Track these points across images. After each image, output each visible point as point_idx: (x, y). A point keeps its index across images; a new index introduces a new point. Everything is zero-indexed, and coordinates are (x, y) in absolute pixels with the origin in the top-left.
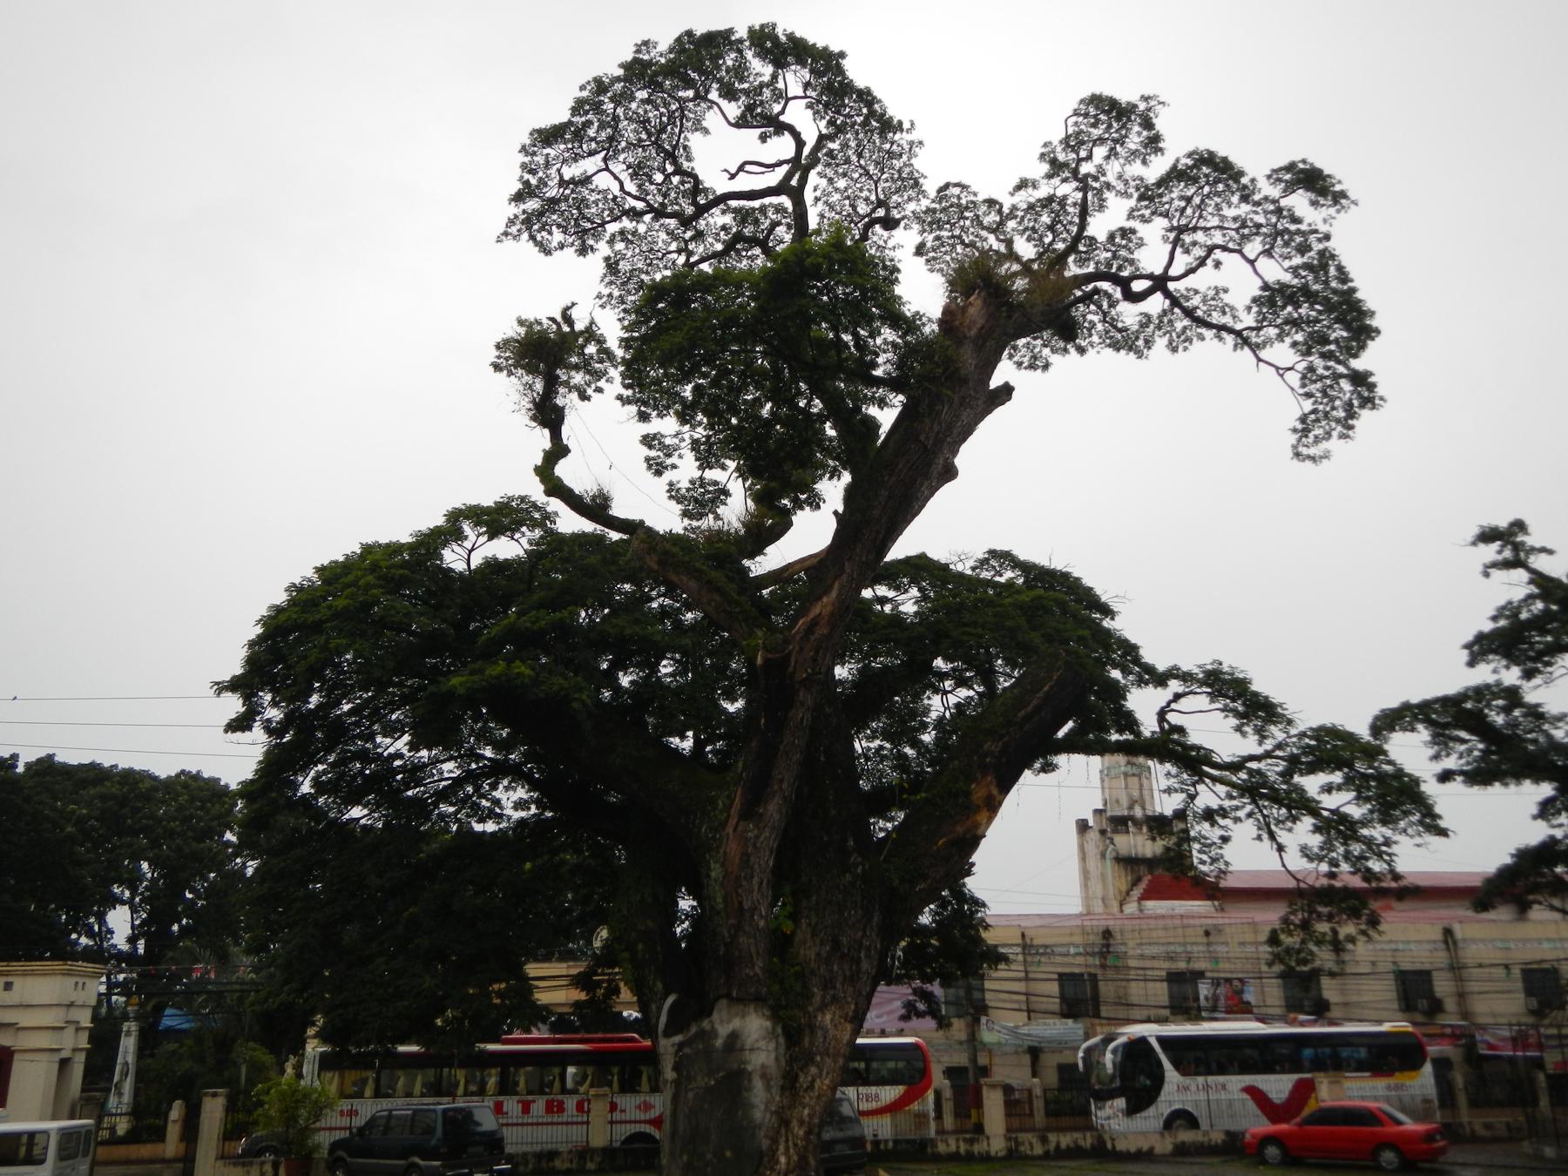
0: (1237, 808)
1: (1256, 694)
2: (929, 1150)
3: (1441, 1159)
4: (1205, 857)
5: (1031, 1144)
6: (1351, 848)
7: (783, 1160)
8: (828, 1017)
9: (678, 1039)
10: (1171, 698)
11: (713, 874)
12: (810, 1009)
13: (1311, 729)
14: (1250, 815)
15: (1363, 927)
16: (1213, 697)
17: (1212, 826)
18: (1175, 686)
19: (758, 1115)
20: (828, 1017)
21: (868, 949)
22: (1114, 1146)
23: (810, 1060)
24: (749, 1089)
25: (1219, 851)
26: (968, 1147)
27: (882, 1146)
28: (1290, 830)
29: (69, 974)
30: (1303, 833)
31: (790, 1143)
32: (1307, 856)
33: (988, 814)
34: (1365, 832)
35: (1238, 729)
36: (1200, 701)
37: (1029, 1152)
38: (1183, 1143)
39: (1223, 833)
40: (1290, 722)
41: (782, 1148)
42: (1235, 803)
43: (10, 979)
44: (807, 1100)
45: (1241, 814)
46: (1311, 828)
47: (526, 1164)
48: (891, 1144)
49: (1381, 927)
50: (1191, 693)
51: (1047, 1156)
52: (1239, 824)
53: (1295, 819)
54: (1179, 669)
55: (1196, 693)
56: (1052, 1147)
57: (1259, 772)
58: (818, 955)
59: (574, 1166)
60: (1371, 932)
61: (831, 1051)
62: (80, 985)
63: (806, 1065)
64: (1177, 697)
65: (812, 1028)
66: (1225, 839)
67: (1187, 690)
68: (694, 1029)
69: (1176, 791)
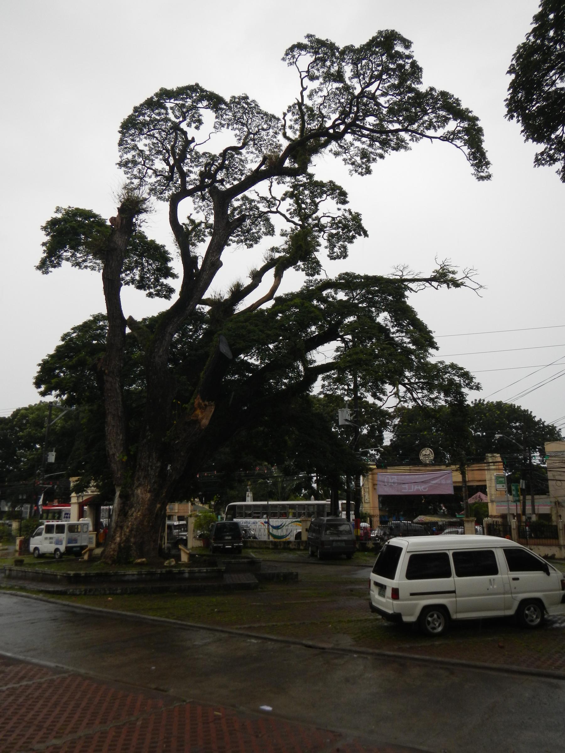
7: (118, 539)
8: (139, 491)
20: (139, 491)
21: (151, 466)
23: (132, 506)
31: (123, 534)
41: (118, 535)
44: (130, 519)
47: (280, 545)
59: (296, 547)
61: (140, 503)
65: (133, 494)
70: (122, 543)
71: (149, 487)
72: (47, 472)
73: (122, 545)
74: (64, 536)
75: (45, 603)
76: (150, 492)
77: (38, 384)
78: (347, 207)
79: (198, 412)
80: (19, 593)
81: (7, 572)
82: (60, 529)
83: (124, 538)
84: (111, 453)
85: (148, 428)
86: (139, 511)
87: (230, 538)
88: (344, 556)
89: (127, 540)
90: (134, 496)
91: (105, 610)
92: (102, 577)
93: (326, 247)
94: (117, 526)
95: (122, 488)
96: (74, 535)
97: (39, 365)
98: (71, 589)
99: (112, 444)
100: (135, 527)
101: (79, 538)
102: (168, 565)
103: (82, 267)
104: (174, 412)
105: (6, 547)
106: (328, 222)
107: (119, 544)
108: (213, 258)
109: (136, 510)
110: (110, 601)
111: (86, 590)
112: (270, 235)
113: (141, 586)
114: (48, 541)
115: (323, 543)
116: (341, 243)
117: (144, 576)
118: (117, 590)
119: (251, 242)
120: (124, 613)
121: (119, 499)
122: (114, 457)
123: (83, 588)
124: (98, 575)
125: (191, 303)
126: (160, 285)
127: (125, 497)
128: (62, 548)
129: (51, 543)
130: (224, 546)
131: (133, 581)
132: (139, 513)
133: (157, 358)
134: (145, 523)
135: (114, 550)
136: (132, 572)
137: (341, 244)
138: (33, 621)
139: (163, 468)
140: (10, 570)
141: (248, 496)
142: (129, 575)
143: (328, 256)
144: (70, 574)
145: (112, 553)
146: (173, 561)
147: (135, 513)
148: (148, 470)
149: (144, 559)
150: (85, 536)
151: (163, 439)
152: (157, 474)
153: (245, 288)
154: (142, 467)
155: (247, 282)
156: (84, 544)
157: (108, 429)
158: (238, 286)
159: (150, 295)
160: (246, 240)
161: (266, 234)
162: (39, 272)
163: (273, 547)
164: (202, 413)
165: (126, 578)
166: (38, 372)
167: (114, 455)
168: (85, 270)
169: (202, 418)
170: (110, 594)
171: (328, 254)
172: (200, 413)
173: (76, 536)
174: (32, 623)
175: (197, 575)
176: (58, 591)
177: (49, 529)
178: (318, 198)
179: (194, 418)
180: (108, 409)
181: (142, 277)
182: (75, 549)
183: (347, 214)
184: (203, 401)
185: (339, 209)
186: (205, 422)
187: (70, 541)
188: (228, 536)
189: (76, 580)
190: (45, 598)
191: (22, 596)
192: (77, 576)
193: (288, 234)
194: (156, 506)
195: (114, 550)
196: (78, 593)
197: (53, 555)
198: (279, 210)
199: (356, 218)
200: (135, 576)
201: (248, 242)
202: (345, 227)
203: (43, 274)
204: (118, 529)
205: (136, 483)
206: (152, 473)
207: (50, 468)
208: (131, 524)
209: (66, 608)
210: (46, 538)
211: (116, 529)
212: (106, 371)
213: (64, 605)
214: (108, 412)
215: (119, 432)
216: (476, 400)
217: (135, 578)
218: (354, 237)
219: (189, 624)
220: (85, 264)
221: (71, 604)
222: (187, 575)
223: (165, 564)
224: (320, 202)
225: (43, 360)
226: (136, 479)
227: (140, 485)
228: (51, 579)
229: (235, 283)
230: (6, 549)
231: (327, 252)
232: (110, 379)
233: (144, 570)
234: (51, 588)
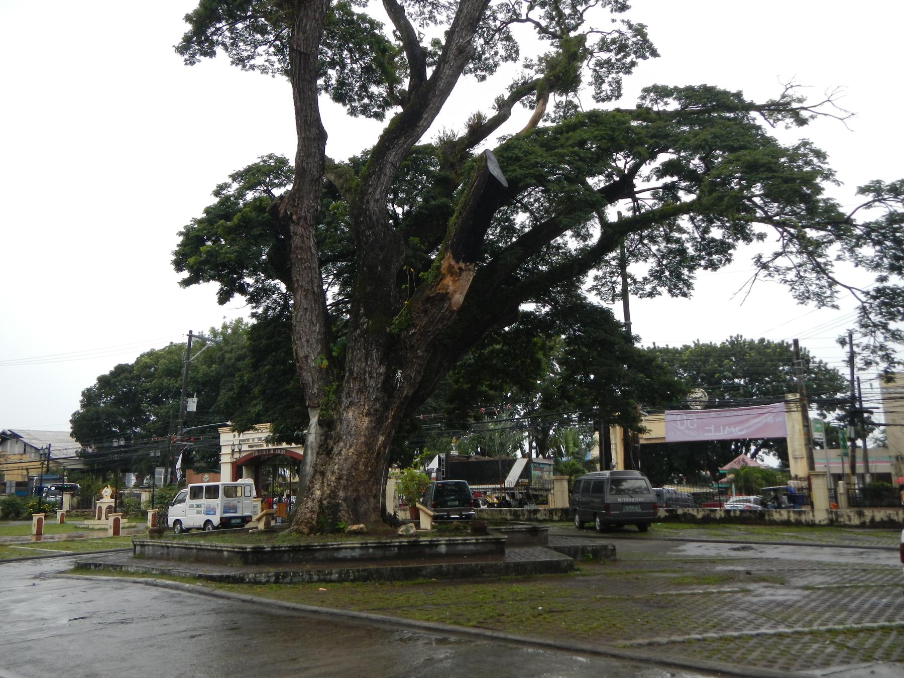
2: (767, 518)
5: (849, 517)
8: (350, 414)
12: (341, 410)
20: (350, 414)
21: (370, 373)
23: (339, 439)
26: (796, 516)
27: (732, 514)
31: (325, 484)
37: (847, 522)
41: (317, 486)
47: (524, 515)
48: (738, 513)
51: (863, 525)
56: (868, 520)
59: (547, 518)
61: (353, 433)
63: (338, 441)
70: (325, 499)
71: (367, 407)
72: (185, 424)
73: (325, 502)
74: (218, 503)
75: (209, 598)
76: (368, 415)
77: (179, 265)
78: (625, 15)
79: (448, 281)
80: (159, 581)
81: (138, 548)
82: (212, 492)
83: (328, 492)
84: (302, 354)
86: (351, 446)
87: (457, 503)
88: (634, 528)
89: (333, 495)
90: (341, 423)
91: (325, 609)
92: (300, 553)
93: (590, 84)
94: (315, 471)
95: (322, 410)
96: (232, 501)
97: (181, 234)
98: (251, 573)
99: (304, 340)
100: (345, 472)
101: (239, 505)
102: (404, 533)
103: (247, 67)
104: (404, 286)
105: (133, 524)
106: (594, 44)
107: (320, 501)
108: (461, 41)
109: (346, 445)
110: (323, 592)
111: (277, 575)
112: (512, 59)
113: (372, 567)
114: (194, 510)
115: (607, 507)
116: (614, 75)
117: (371, 550)
118: (331, 574)
119: (483, 73)
120: (363, 615)
121: (318, 427)
122: (307, 360)
123: (272, 571)
124: (295, 550)
125: (425, 116)
126: (369, 97)
127: (327, 424)
128: (216, 520)
129: (198, 513)
130: (448, 515)
131: (353, 560)
132: (352, 450)
133: (372, 204)
134: (362, 467)
135: (312, 512)
136: (350, 546)
137: (613, 78)
138: (194, 633)
139: (389, 377)
140: (142, 546)
142: (346, 548)
143: (594, 97)
144: (246, 548)
145: (309, 515)
146: (412, 527)
147: (344, 450)
148: (365, 379)
149: (362, 526)
150: (247, 502)
151: (388, 329)
152: (379, 386)
153: (490, 120)
154: (355, 375)
155: (490, 113)
156: (246, 514)
157: (296, 316)
158: (479, 117)
159: (353, 112)
160: (476, 70)
161: (505, 59)
162: (180, 59)
163: (512, 517)
164: (454, 281)
165: (341, 554)
166: (178, 246)
167: (306, 357)
168: (251, 71)
169: (455, 292)
170: (319, 581)
171: (594, 94)
172: (451, 283)
173: (235, 502)
174: (192, 637)
175: (460, 548)
176: (228, 577)
177: (196, 493)
178: (582, 5)
179: (441, 291)
180: (298, 281)
181: (341, 83)
182: (233, 521)
183: (624, 28)
184: (457, 262)
185: (614, 21)
186: (458, 298)
187: (226, 509)
188: (454, 500)
189: (257, 557)
190: (205, 589)
191: (165, 586)
192: (257, 551)
193: (533, 66)
194: (378, 440)
195: (312, 512)
196: (264, 580)
198: (530, 16)
199: (639, 31)
200: (357, 550)
201: (479, 73)
202: (622, 48)
203: (186, 64)
204: (318, 476)
205: (345, 402)
206: (372, 383)
207: (191, 419)
208: (338, 469)
209: (249, 606)
210: (191, 506)
211: (313, 477)
212: (294, 217)
213: (244, 601)
214: (296, 286)
215: (314, 319)
216: (731, 337)
217: (356, 553)
218: (633, 64)
219: (511, 636)
220: (252, 62)
221: (256, 599)
222: (443, 549)
223: (400, 533)
224: (584, 10)
225: (185, 227)
226: (344, 394)
227: (352, 404)
228: (215, 557)
229: (475, 112)
230: (134, 527)
231: (592, 90)
232: (300, 230)
233: (371, 541)
234: (216, 571)
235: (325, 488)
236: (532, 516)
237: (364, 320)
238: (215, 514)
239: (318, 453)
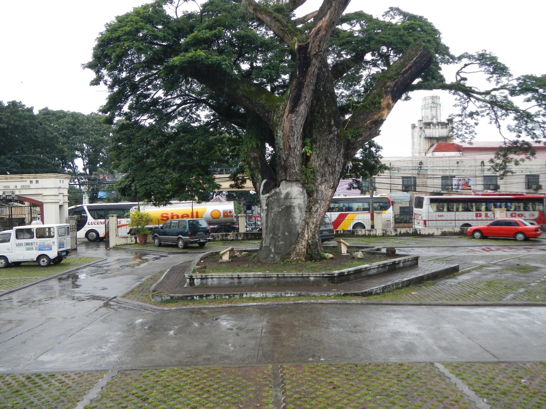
0: (483, 112)
1: (500, 63)
2: (355, 234)
3: (539, 237)
4: (467, 131)
5: (391, 232)
6: (528, 126)
7: (306, 236)
8: (323, 187)
9: (267, 195)
10: (463, 66)
11: (279, 135)
12: (316, 184)
13: (523, 76)
14: (488, 114)
15: (528, 156)
16: (481, 65)
17: (472, 119)
18: (465, 61)
19: (297, 221)
20: (323, 187)
21: (339, 162)
22: (420, 232)
23: (316, 202)
24: (294, 212)
25: (473, 129)
26: (369, 232)
27: (339, 232)
28: (504, 120)
29: (56, 177)
30: (510, 120)
31: (309, 230)
32: (509, 129)
33: (387, 111)
34: (535, 119)
35: (488, 79)
36: (475, 67)
37: (390, 234)
38: (445, 232)
39: (476, 121)
40: (510, 75)
41: (306, 232)
42: (483, 109)
43: (37, 179)
44: (315, 216)
45: (485, 114)
46: (513, 118)
47: (218, 237)
48: (342, 232)
49: (536, 156)
50: (471, 63)
51: (396, 235)
52: (483, 117)
53: (507, 115)
54: (467, 54)
55: (474, 64)
56: (398, 233)
57: (495, 96)
58: (320, 165)
59: (234, 238)
60: (531, 157)
62: (62, 181)
64: (466, 65)
66: (476, 124)
67: (470, 62)
68: (273, 192)
69: (458, 106)
70: (310, 240)
73: (309, 241)
85: (333, 122)
90: (317, 192)
129: (28, 249)
132: (323, 209)
141: (85, 198)
197: (37, 264)
200: (376, 269)
235: (310, 233)
236: (224, 238)
237: (334, 128)
238: (51, 249)
239: (306, 211)
